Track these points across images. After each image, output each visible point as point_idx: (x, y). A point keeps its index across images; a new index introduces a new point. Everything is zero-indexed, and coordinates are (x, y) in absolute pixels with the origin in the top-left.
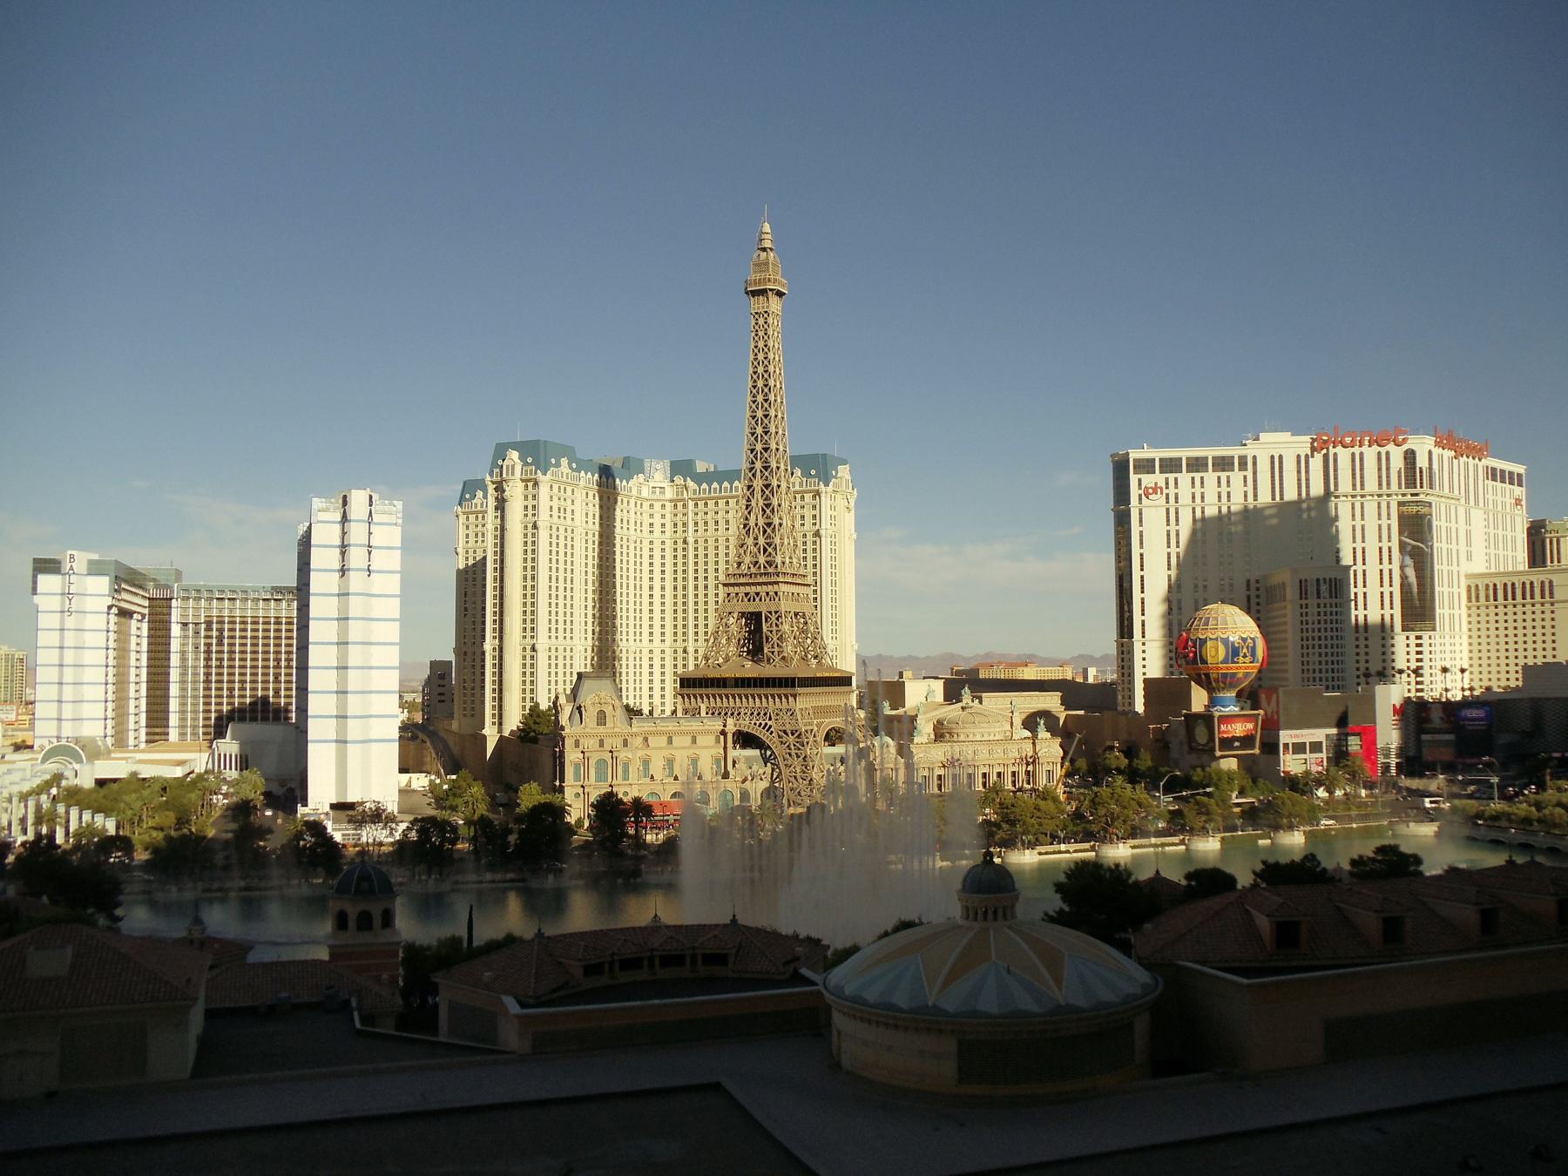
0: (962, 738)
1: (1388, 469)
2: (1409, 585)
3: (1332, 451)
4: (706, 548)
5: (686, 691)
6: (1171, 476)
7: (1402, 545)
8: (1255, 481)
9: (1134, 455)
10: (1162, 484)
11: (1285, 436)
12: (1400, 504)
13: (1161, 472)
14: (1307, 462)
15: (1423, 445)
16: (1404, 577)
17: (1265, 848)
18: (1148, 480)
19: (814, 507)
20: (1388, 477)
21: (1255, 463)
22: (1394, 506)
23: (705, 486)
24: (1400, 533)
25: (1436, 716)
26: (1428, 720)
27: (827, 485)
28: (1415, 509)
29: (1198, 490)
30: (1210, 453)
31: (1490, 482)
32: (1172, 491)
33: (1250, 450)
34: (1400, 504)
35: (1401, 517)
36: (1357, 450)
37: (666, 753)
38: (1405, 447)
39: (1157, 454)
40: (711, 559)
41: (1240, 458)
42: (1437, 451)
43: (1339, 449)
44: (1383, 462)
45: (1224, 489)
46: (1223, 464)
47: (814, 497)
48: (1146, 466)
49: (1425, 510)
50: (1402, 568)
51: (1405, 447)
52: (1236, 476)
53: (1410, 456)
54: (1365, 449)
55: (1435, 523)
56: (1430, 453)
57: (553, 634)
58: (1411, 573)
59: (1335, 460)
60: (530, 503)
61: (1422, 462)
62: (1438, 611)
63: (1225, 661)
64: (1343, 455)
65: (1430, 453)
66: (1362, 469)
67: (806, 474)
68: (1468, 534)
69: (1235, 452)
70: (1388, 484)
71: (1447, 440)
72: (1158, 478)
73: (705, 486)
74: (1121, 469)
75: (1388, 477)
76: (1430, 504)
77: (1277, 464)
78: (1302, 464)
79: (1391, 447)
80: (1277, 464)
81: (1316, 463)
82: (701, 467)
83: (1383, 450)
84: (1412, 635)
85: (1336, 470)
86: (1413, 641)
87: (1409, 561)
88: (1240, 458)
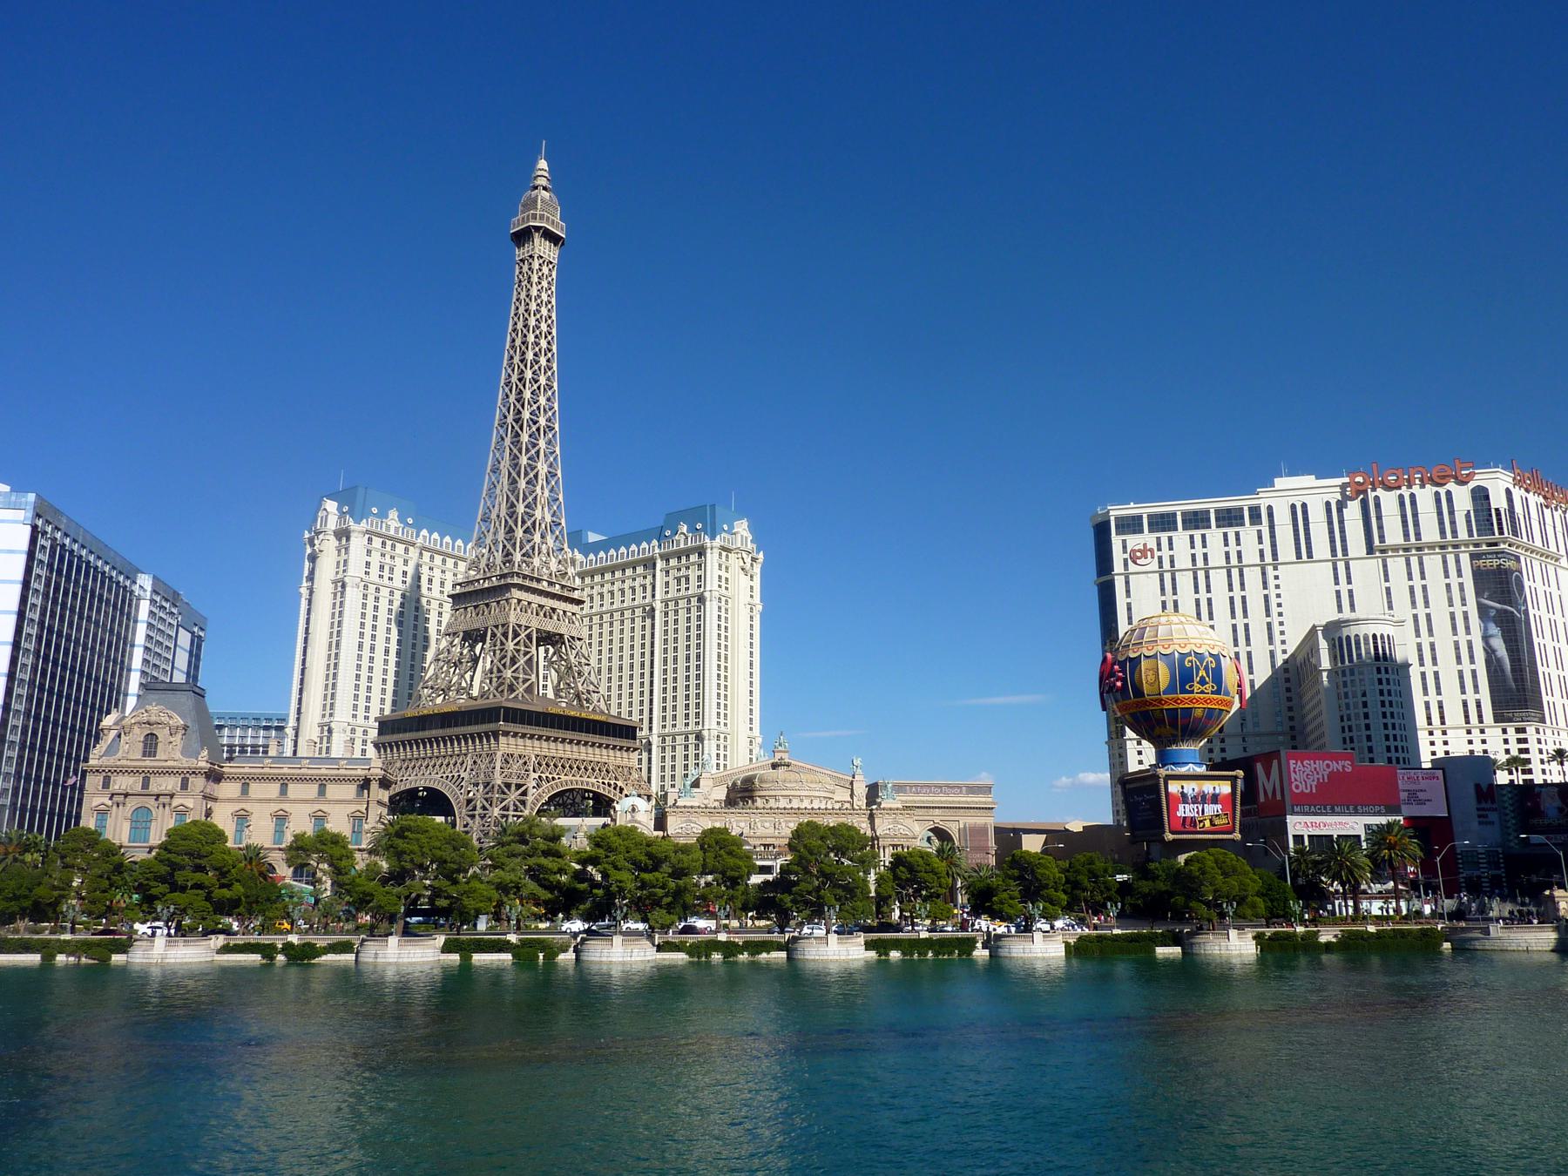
0: (759, 802)
1: (1452, 512)
2: (1499, 660)
3: (1371, 495)
4: (621, 640)
5: (387, 738)
6: (1164, 536)
7: (1483, 610)
9: (1116, 512)
10: (1152, 544)
11: (1309, 480)
13: (1151, 531)
14: (1340, 511)
15: (1498, 483)
16: (1490, 652)
17: (1169, 962)
18: (1134, 541)
20: (1453, 523)
22: (1465, 559)
23: (592, 556)
24: (1478, 594)
25: (1550, 805)
26: (1537, 812)
27: (713, 538)
28: (1496, 562)
29: (1199, 550)
30: (1212, 505)
32: (1166, 553)
33: (1263, 499)
34: (1473, 556)
35: (1478, 574)
36: (1405, 491)
37: (274, 807)
38: (1472, 485)
39: (1145, 510)
40: (681, 683)
42: (1518, 493)
43: (1380, 492)
44: (1445, 506)
45: (1233, 548)
46: (1230, 518)
47: (700, 555)
48: (1131, 525)
49: (1511, 564)
50: (1486, 638)
51: (1472, 485)
52: (1248, 532)
53: (1481, 496)
54: (1416, 489)
55: (1527, 584)
56: (1508, 492)
57: (361, 713)
58: (1502, 651)
59: (1378, 506)
60: (343, 557)
61: (1498, 501)
62: (1545, 699)
63: (1171, 688)
64: (1389, 500)
65: (1508, 492)
66: (1415, 515)
67: (693, 529)
69: (1244, 502)
70: (1454, 533)
71: (1532, 478)
72: (1147, 538)
73: (592, 556)
75: (1453, 523)
76: (1518, 559)
77: (1299, 515)
78: (1334, 514)
79: (1451, 486)
80: (1299, 515)
81: (1353, 510)
82: (593, 537)
83: (1442, 491)
85: (1379, 518)
86: (1512, 735)
87: (1494, 630)
88: (1251, 509)
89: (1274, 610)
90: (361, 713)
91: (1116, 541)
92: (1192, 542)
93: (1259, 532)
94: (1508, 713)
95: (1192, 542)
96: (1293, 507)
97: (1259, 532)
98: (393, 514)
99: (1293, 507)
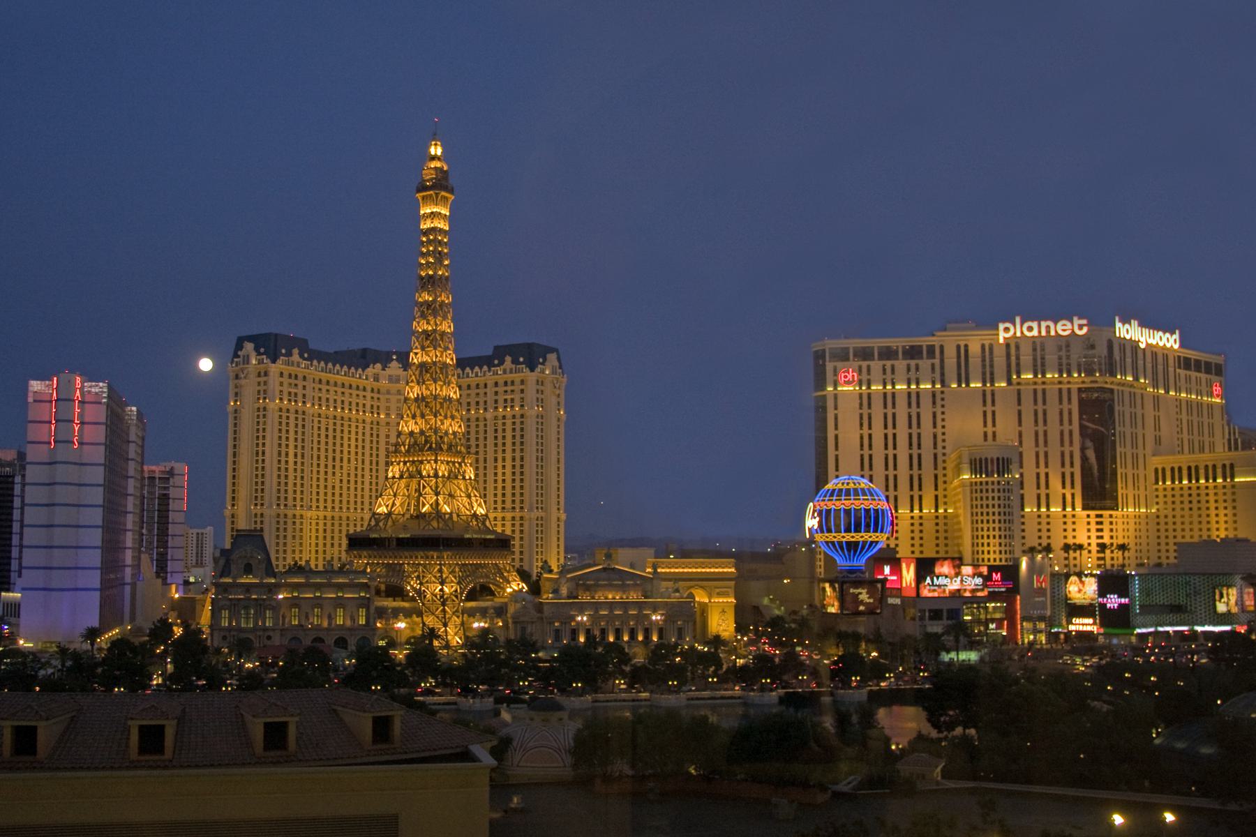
6: (864, 364)
7: (1082, 427)
8: (942, 367)
12: (1080, 390)
16: (1084, 459)
19: (522, 391)
21: (942, 352)
27: (532, 370)
31: (1182, 372)
35: (1081, 401)
41: (928, 346)
50: (1083, 449)
58: (1091, 454)
68: (1157, 420)
74: (820, 356)
84: (1093, 513)
87: (1089, 444)
89: (939, 424)
90: (282, 502)
91: (829, 366)
92: (884, 370)
93: (933, 365)
94: (1092, 504)
95: (884, 370)
96: (958, 347)
97: (933, 365)
98: (296, 351)
99: (958, 347)
